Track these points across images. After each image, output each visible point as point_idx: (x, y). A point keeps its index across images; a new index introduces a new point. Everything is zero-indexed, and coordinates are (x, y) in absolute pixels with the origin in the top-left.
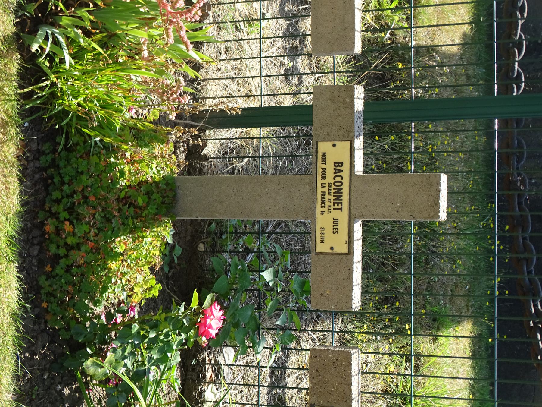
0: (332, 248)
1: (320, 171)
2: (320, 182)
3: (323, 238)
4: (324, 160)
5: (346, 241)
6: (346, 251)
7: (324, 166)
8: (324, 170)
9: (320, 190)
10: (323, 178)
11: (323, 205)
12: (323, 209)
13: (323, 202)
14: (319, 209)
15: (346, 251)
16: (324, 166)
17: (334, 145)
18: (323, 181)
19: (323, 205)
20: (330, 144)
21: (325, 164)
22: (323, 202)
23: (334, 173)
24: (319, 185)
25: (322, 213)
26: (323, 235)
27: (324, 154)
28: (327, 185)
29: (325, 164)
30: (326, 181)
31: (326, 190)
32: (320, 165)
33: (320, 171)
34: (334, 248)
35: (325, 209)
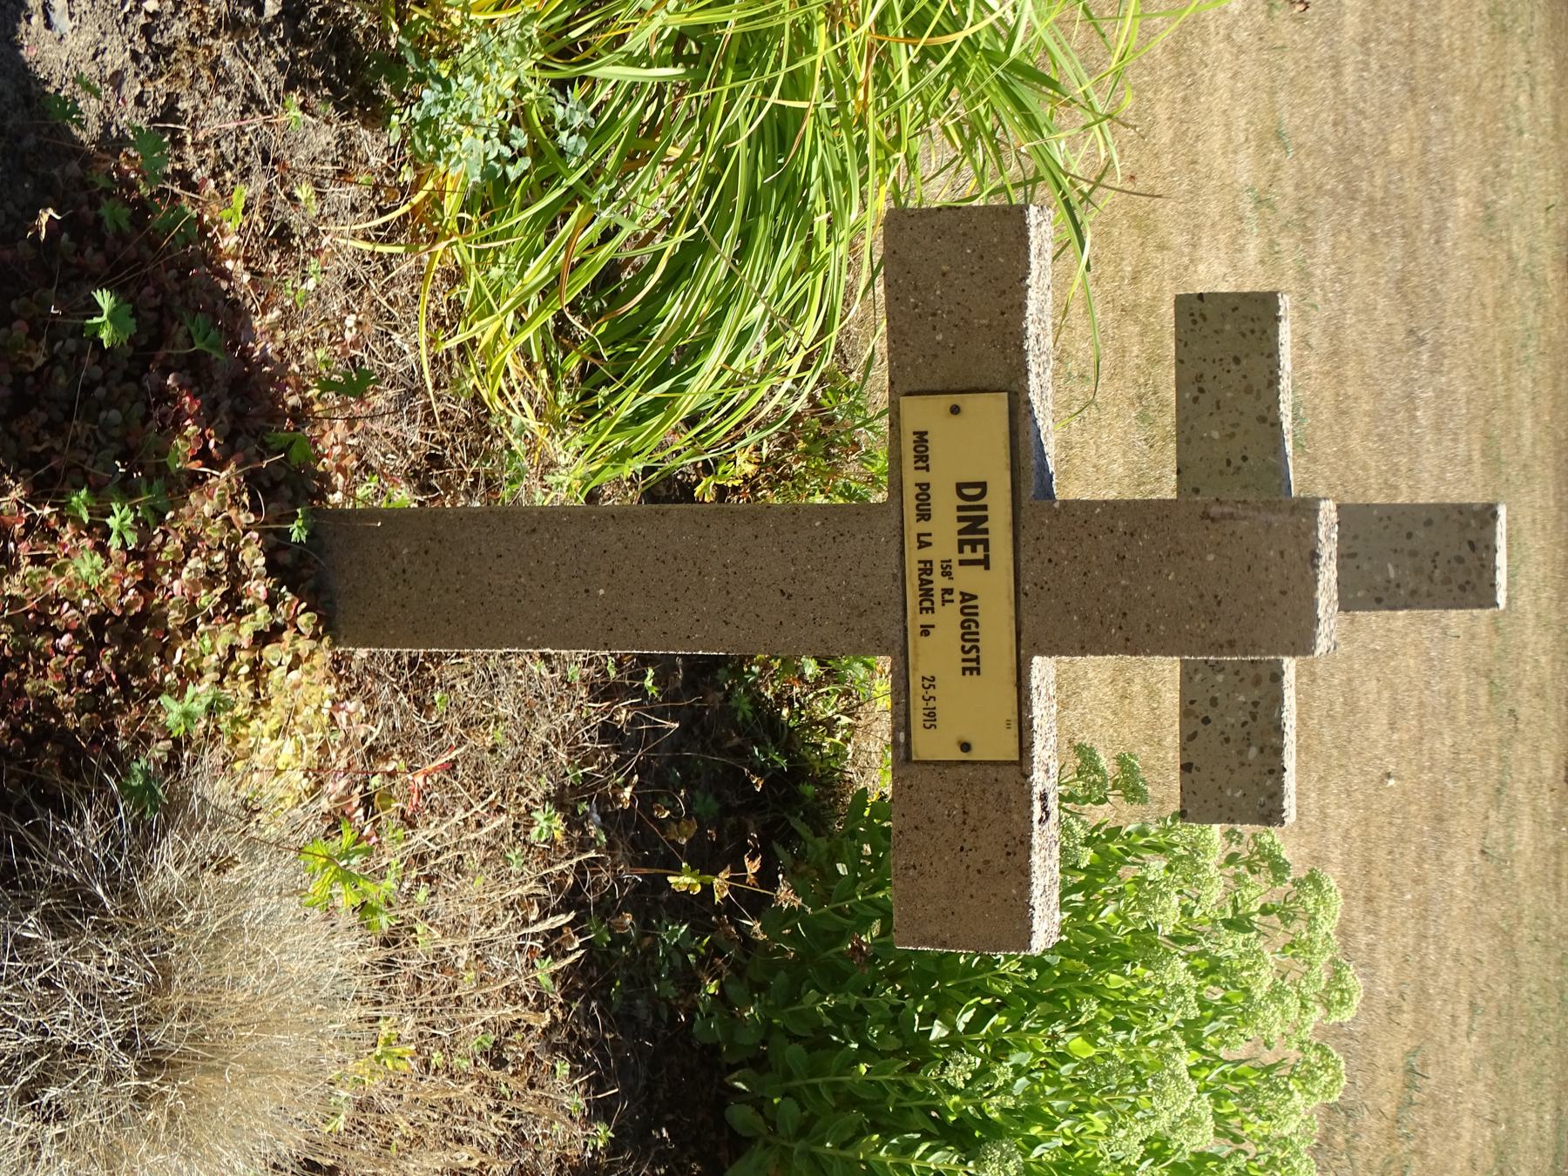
0: (966, 747)
1: (910, 492)
2: (913, 527)
3: (931, 715)
4: (922, 458)
5: (1008, 723)
6: (1010, 752)
7: (922, 477)
8: (924, 487)
9: (914, 556)
10: (924, 515)
11: (927, 604)
12: (926, 619)
13: (927, 594)
14: (915, 620)
15: (1010, 752)
16: (922, 477)
17: (955, 410)
18: (924, 527)
19: (927, 604)
21: (927, 468)
22: (927, 594)
24: (911, 542)
25: (926, 631)
26: (931, 704)
27: (921, 437)
29: (927, 468)
32: (911, 477)
33: (910, 492)
34: (974, 746)
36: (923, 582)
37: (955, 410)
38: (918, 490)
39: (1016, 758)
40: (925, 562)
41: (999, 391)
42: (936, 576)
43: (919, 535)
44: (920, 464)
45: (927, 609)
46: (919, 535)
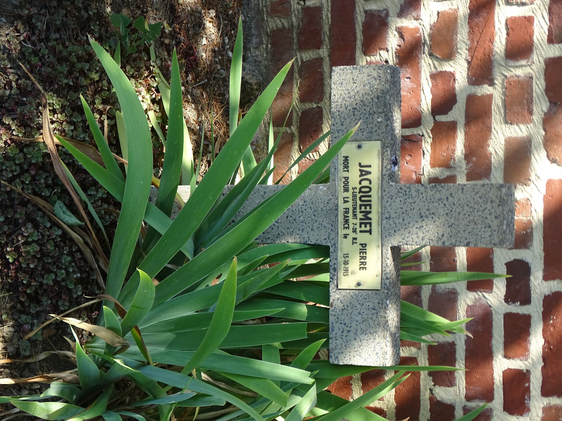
2: (342, 195)
4: (346, 167)
7: (346, 174)
8: (347, 179)
10: (346, 190)
11: (346, 226)
12: (346, 231)
13: (347, 221)
16: (346, 174)
18: (346, 195)
19: (346, 226)
20: (355, 145)
21: (348, 171)
23: (360, 176)
24: (341, 201)
25: (345, 236)
27: (346, 159)
28: (350, 199)
29: (348, 171)
30: (349, 194)
31: (350, 205)
35: (349, 231)
36: (345, 217)
37: (359, 147)
38: (344, 180)
39: (380, 288)
40: (346, 209)
41: (378, 140)
42: (350, 214)
43: (344, 198)
44: (345, 169)
45: (346, 228)
46: (344, 198)
